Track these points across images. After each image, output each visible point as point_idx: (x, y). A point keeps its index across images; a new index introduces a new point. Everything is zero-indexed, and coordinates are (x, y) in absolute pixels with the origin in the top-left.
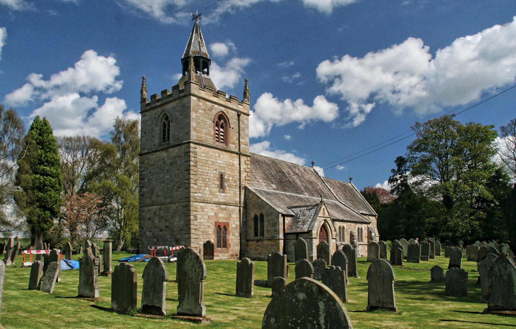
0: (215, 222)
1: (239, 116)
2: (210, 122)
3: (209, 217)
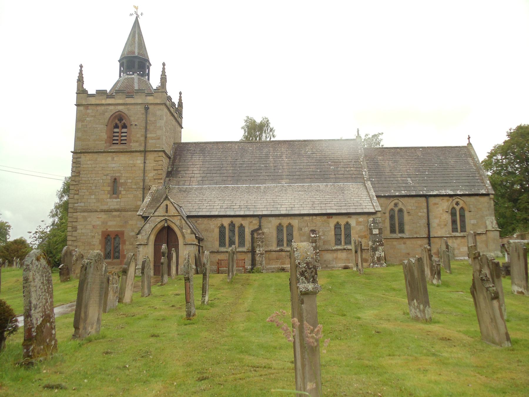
0: (103, 233)
1: (147, 109)
2: (102, 126)
3: (94, 227)
